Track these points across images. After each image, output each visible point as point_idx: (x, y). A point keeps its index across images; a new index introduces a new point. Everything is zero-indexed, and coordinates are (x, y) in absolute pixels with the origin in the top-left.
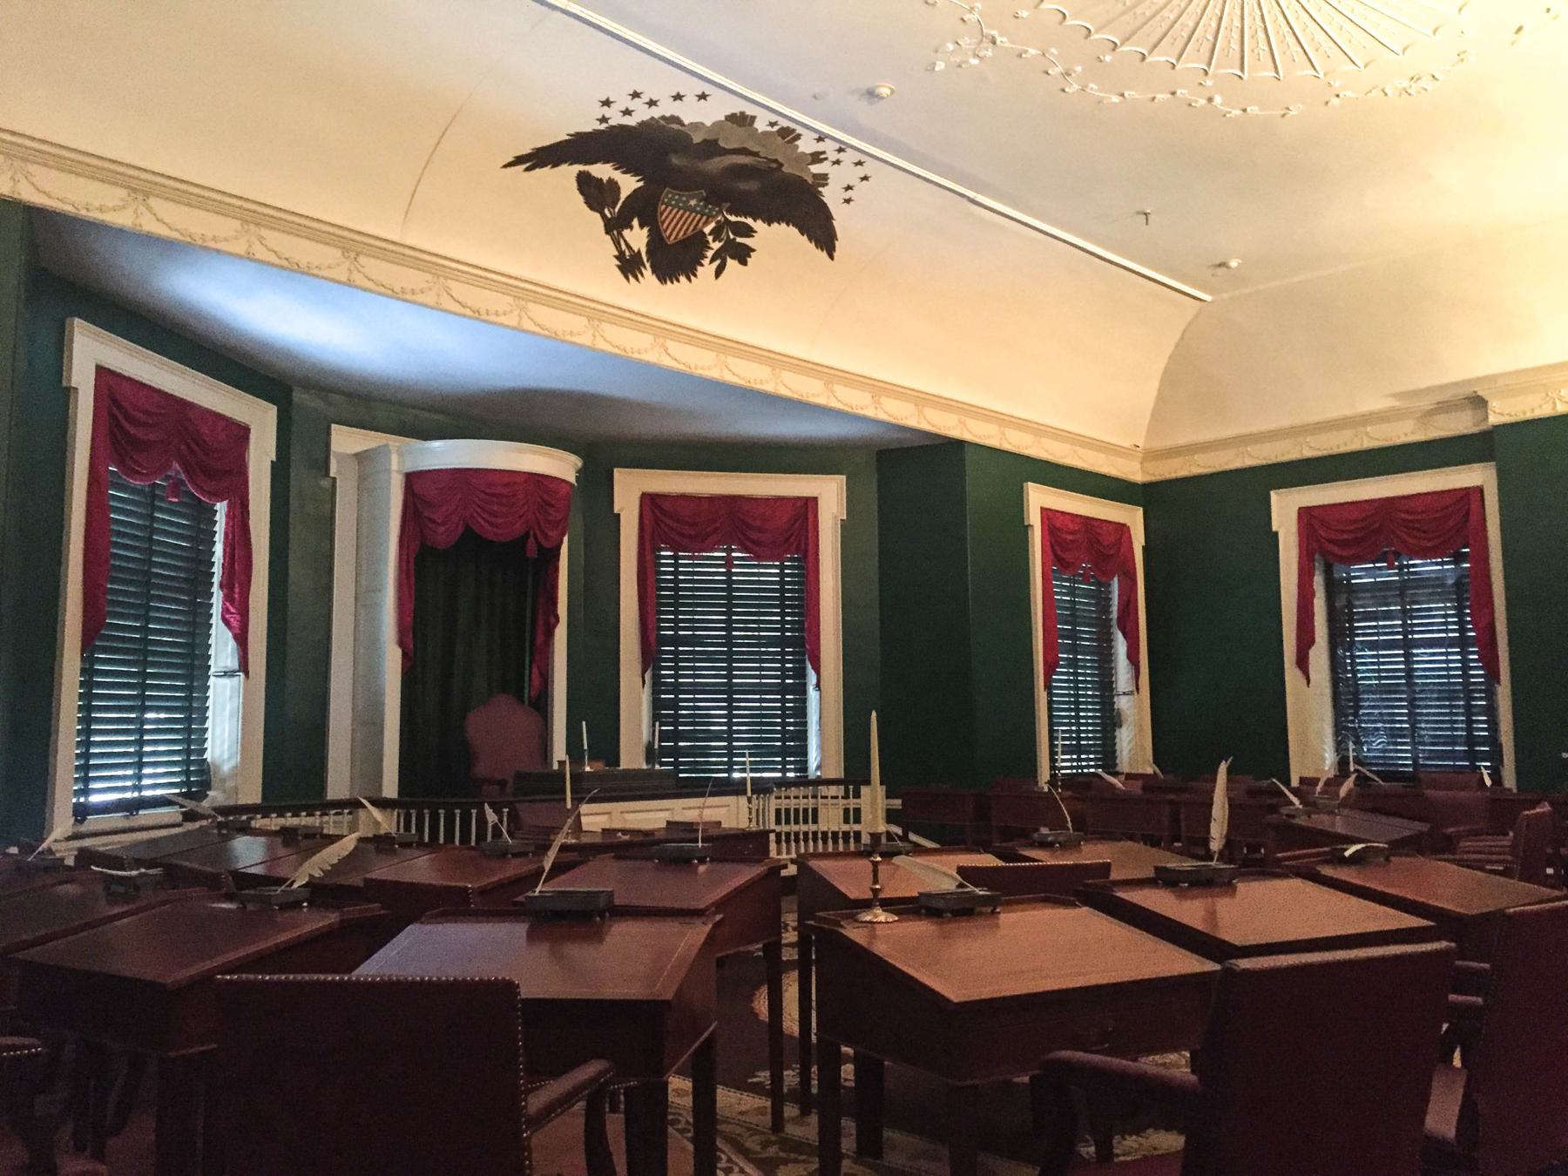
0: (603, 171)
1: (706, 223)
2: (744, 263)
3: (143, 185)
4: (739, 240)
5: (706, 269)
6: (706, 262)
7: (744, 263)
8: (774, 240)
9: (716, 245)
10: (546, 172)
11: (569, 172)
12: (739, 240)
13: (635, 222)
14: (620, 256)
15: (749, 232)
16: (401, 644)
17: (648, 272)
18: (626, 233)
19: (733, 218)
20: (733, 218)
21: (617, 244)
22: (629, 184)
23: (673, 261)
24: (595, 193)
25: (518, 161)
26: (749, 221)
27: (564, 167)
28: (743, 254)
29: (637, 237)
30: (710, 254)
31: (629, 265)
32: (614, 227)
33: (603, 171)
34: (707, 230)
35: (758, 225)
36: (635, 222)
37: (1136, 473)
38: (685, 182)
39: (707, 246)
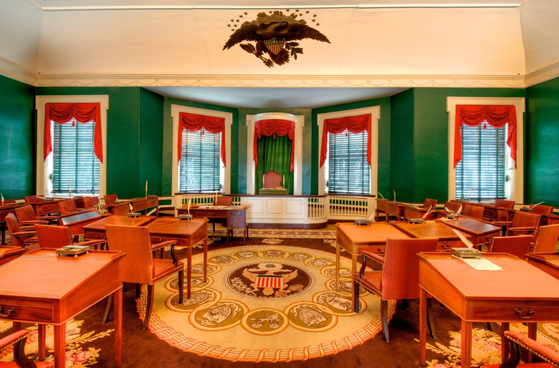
0: (245, 42)
1: (282, 46)
2: (302, 53)
3: (157, 77)
4: (296, 47)
5: (291, 58)
6: (290, 56)
7: (302, 53)
8: (304, 43)
9: (290, 51)
10: (232, 48)
11: (237, 46)
12: (296, 47)
13: (263, 52)
14: (265, 62)
15: (297, 44)
16: (254, 160)
17: (275, 64)
18: (262, 55)
19: (289, 42)
20: (289, 42)
21: (262, 59)
22: (254, 43)
23: (280, 58)
24: (248, 48)
25: (225, 47)
26: (294, 41)
27: (235, 45)
28: (300, 51)
29: (266, 56)
30: (290, 54)
31: (268, 63)
32: (259, 55)
33: (245, 42)
34: (284, 47)
35: (297, 41)
36: (263, 52)
37: (522, 84)
38: (269, 37)
39: (287, 52)
